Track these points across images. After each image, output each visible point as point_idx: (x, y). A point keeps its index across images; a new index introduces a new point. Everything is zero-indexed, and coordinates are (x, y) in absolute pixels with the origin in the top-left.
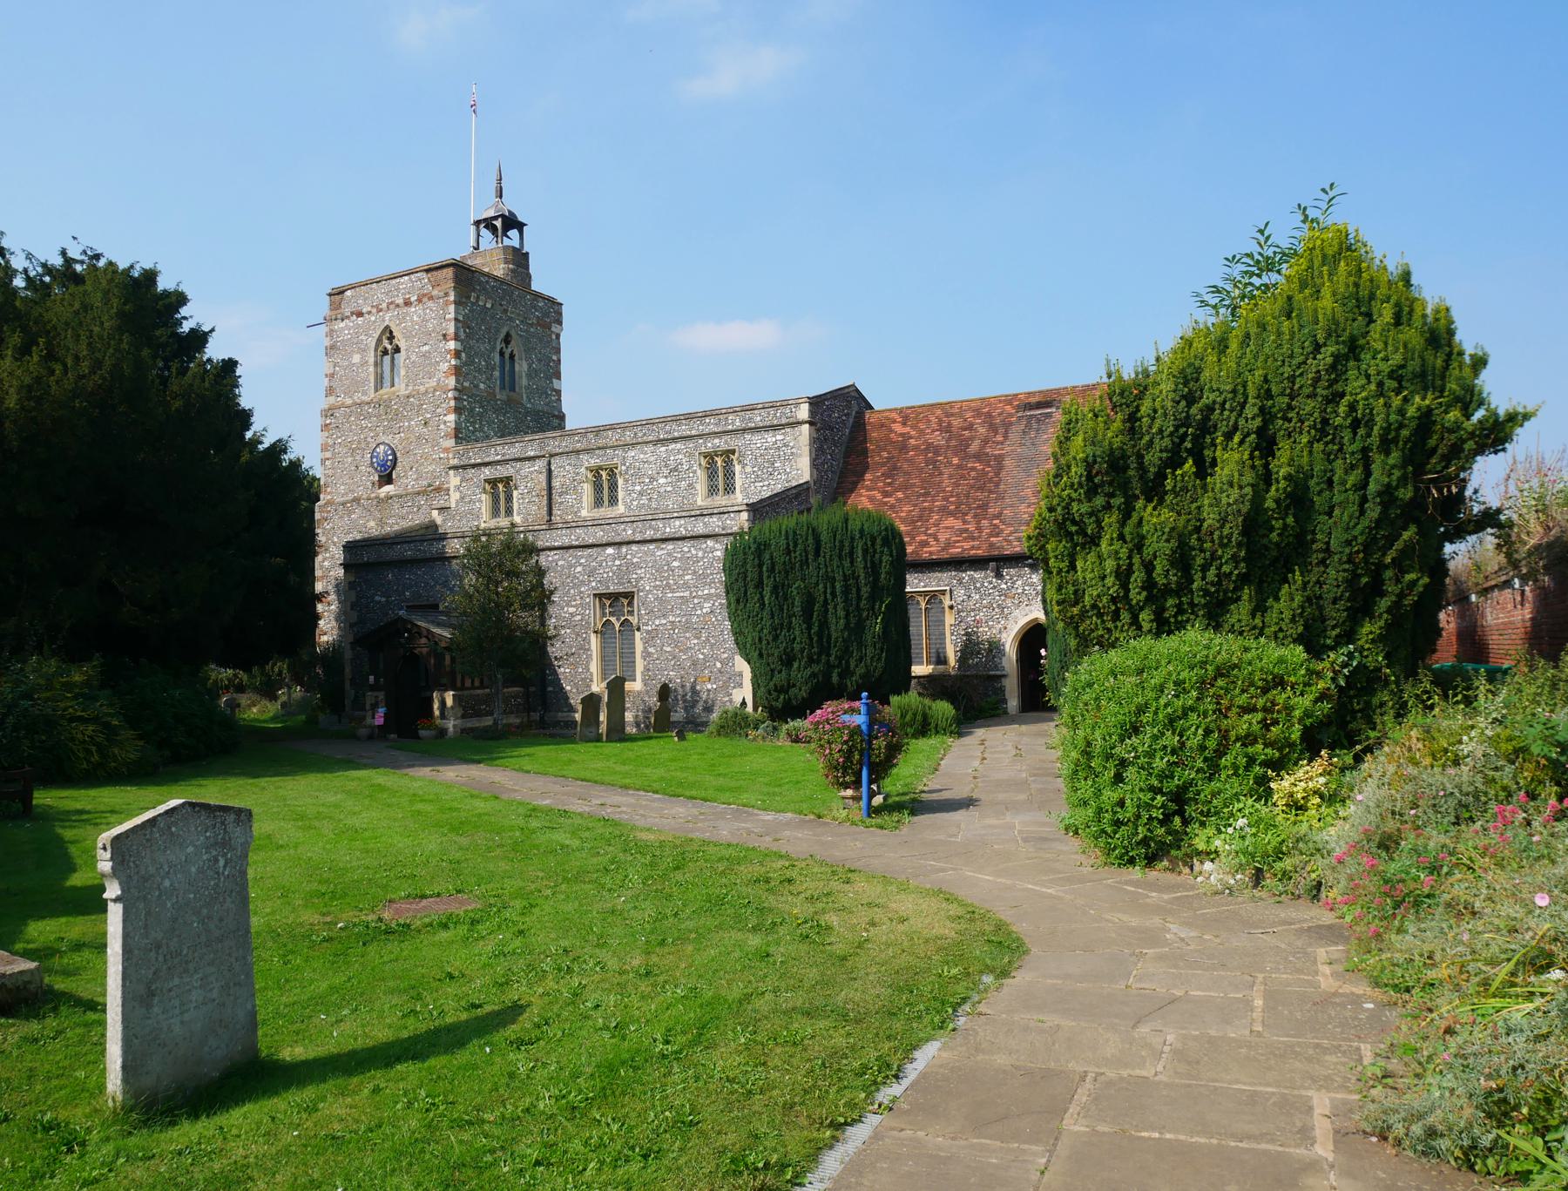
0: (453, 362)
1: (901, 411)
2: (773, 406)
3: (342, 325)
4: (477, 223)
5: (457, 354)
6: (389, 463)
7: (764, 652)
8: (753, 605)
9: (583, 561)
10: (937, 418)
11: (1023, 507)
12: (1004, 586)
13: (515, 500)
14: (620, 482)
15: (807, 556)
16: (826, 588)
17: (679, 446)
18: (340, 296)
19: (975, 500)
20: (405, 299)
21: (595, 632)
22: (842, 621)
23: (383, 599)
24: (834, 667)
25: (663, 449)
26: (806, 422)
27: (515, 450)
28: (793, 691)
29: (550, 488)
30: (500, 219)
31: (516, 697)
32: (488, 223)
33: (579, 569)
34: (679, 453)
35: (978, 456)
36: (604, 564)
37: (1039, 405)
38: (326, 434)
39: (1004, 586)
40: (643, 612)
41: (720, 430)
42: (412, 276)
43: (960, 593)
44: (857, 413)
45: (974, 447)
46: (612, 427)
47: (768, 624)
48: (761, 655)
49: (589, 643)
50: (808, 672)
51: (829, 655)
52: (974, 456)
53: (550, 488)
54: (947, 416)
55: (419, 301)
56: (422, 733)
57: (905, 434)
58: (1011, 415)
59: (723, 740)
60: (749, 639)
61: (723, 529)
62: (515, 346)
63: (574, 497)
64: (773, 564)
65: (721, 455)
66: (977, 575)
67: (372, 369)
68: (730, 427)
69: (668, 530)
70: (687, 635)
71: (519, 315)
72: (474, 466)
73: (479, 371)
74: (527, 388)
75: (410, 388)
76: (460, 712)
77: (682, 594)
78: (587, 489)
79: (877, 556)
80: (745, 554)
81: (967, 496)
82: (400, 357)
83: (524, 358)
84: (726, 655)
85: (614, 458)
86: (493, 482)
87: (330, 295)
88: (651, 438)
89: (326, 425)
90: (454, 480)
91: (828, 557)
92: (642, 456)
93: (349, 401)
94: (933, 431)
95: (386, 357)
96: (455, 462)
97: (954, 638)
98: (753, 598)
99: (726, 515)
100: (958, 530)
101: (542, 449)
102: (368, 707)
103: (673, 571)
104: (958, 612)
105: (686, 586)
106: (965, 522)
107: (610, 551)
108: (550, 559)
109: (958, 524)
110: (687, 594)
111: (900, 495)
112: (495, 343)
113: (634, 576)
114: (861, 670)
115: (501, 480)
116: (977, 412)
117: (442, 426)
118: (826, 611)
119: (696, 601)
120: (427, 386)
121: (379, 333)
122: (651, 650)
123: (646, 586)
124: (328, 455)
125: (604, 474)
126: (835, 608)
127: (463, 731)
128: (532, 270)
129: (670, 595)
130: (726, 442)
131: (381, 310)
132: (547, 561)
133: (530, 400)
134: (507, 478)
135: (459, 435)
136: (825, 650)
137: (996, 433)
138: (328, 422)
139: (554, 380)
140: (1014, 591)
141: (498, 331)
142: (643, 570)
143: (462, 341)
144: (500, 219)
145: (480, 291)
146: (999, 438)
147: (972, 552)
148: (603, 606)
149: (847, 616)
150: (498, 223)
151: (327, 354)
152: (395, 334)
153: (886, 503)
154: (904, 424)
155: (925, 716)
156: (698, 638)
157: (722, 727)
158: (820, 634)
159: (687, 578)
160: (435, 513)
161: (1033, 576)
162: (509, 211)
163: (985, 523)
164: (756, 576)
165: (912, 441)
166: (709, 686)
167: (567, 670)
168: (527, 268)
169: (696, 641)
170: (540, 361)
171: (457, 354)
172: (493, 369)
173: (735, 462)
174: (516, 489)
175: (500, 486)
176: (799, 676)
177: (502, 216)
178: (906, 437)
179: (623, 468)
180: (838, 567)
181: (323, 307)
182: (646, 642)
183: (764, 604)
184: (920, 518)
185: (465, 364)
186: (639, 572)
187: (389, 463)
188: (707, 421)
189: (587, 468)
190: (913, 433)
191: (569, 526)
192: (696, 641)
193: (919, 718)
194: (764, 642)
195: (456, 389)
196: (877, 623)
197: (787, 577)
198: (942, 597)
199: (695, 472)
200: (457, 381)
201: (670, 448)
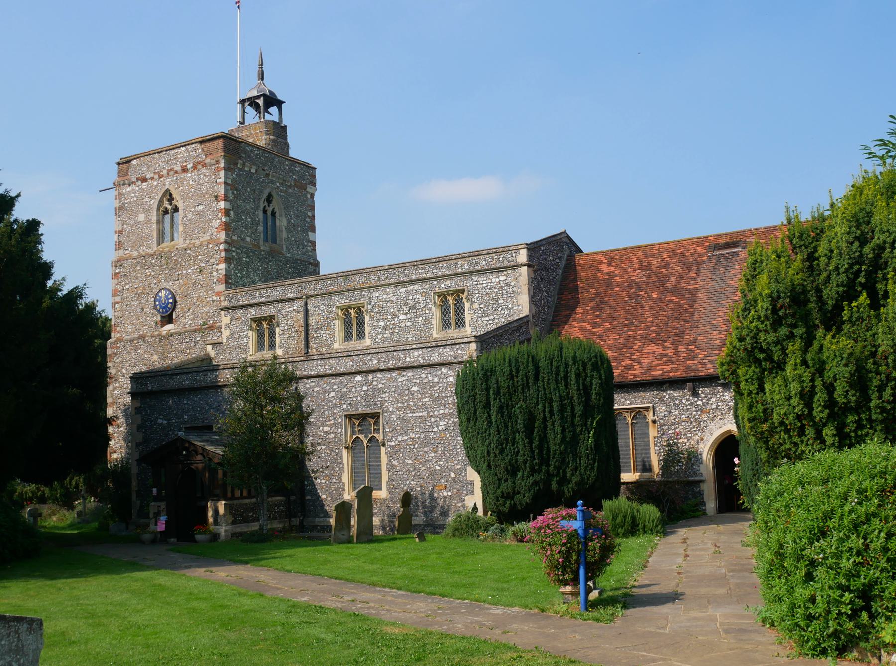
0: (224, 219)
1: (606, 253)
2: (497, 251)
3: (129, 189)
4: (243, 102)
5: (227, 212)
6: (169, 306)
7: (493, 464)
8: (482, 423)
9: (335, 387)
10: (637, 258)
11: (715, 335)
12: (700, 403)
13: (277, 336)
14: (367, 318)
15: (527, 380)
16: (545, 408)
17: (416, 287)
18: (127, 165)
19: (673, 329)
20: (182, 167)
21: (347, 448)
22: (559, 436)
23: (165, 422)
24: (553, 476)
25: (403, 290)
26: (525, 265)
27: (277, 294)
28: (518, 498)
29: (307, 325)
30: (262, 98)
31: (278, 505)
32: (252, 102)
33: (332, 394)
34: (416, 293)
35: (675, 291)
36: (354, 389)
37: (727, 245)
38: (116, 281)
39: (700, 403)
40: (387, 430)
41: (451, 273)
42: (188, 147)
43: (662, 410)
44: (568, 256)
45: (671, 282)
46: (359, 272)
47: (495, 440)
48: (489, 466)
49: (341, 457)
50: (531, 480)
51: (548, 465)
52: (671, 291)
53: (307, 325)
54: (646, 257)
55: (195, 168)
56: (199, 537)
57: (610, 273)
58: (702, 255)
59: (458, 541)
60: (479, 453)
61: (455, 358)
62: (276, 205)
63: (327, 332)
64: (498, 388)
65: (453, 295)
66: (676, 394)
67: (154, 226)
68: (460, 270)
69: (408, 359)
70: (426, 449)
71: (279, 178)
72: (242, 307)
73: (246, 226)
74: (288, 239)
75: (188, 241)
76: (230, 518)
77: (420, 414)
78: (338, 325)
79: (588, 379)
80: (474, 379)
81: (666, 325)
82: (179, 216)
83: (283, 213)
84: (459, 467)
85: (361, 298)
86: (258, 321)
87: (119, 164)
88: (392, 281)
89: (116, 274)
90: (225, 319)
91: (546, 381)
92: (385, 296)
93: (135, 254)
94: (635, 270)
95: (166, 216)
96: (226, 304)
97: (657, 448)
98: (481, 417)
99: (458, 346)
100: (658, 355)
101: (300, 291)
102: (151, 515)
103: (412, 395)
104: (661, 426)
105: (424, 407)
106: (664, 348)
107: (359, 378)
108: (308, 385)
109: (658, 350)
110: (425, 414)
111: (607, 325)
112: (259, 203)
113: (380, 399)
114: (576, 479)
115: (265, 319)
116: (673, 253)
117: (215, 274)
118: (545, 428)
119: (433, 420)
120: (201, 239)
121: (160, 195)
122: (395, 463)
123: (390, 408)
124: (118, 299)
125: (352, 312)
126: (553, 424)
127: (234, 535)
128: (288, 141)
129: (410, 415)
130: (456, 283)
131: (162, 176)
132: (305, 387)
133: (289, 250)
134: (269, 316)
135: (229, 281)
136: (545, 461)
137: (690, 271)
138: (118, 271)
139: (310, 233)
141: (261, 192)
142: (387, 394)
143: (231, 201)
144: (262, 98)
145: (245, 158)
146: (693, 275)
147: (672, 374)
148: (353, 426)
149: (563, 431)
150: (261, 101)
151: (116, 214)
152: (174, 196)
153: (595, 333)
154: (609, 264)
155: (634, 518)
156: (435, 452)
157: (456, 529)
158: (540, 448)
159: (425, 400)
160: (209, 348)
161: (726, 394)
162: (270, 91)
163: (682, 348)
164: (484, 399)
165: (617, 279)
166: (445, 494)
167: (323, 481)
168: (285, 138)
169: (433, 455)
170: (297, 216)
171: (227, 212)
172: (258, 224)
173: (465, 301)
174: (278, 326)
175: (265, 324)
176: (523, 484)
177: (264, 95)
178: (612, 275)
179: (369, 307)
180: (554, 389)
181: (113, 174)
182: (390, 456)
183: (491, 422)
184: (625, 345)
185: (234, 221)
186: (384, 396)
187: (169, 306)
188: (440, 265)
189: (338, 308)
190: (617, 272)
191: (323, 357)
192: (433, 455)
193: (628, 519)
194: (492, 455)
195: (226, 242)
196: (589, 437)
197: (511, 399)
198: (646, 413)
199: (430, 309)
200: (227, 235)
201: (409, 289)
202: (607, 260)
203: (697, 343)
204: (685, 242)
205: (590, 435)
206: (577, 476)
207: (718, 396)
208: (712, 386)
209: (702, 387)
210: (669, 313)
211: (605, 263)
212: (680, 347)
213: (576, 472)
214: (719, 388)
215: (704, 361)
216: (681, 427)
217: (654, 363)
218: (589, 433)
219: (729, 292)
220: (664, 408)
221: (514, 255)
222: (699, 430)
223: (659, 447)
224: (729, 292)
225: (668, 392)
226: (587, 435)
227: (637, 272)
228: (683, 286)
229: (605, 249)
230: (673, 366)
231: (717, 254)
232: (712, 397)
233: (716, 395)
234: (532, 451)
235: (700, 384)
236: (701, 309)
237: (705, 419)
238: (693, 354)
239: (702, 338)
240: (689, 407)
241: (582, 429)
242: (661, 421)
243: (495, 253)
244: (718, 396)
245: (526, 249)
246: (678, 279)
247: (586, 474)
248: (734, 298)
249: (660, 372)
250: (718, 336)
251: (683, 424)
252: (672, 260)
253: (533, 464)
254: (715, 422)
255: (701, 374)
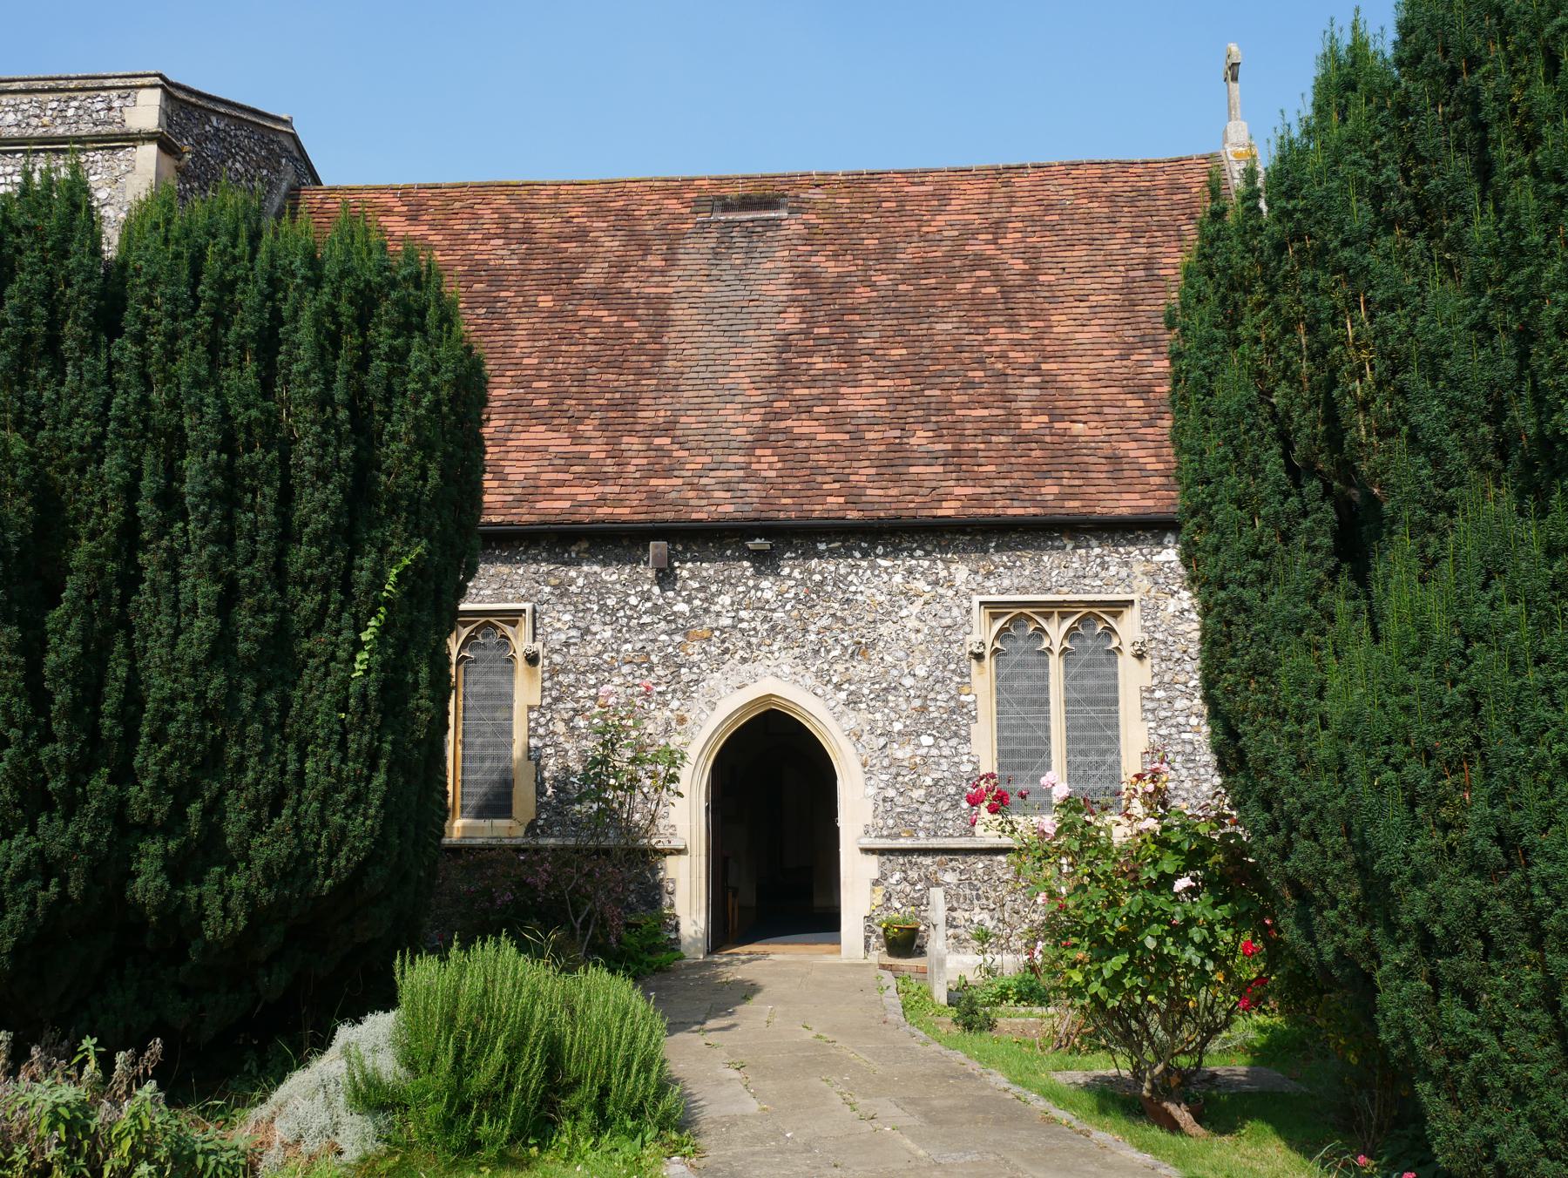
1: (404, 192)
2: (55, 87)
11: (730, 413)
12: (681, 607)
15: (54, 324)
16: (137, 475)
19: (603, 389)
22: (202, 627)
24: (147, 829)
35: (603, 296)
37: (746, 203)
39: (681, 607)
43: (560, 622)
45: (593, 275)
51: (125, 775)
52: (595, 295)
54: (519, 210)
57: (414, 238)
58: (681, 219)
66: (610, 575)
79: (379, 367)
81: (581, 380)
91: (156, 341)
94: (488, 237)
100: (558, 455)
104: (554, 672)
106: (576, 439)
109: (559, 442)
114: (269, 849)
116: (598, 207)
118: (131, 580)
126: (172, 563)
137: (646, 251)
140: (709, 621)
146: (655, 262)
147: (603, 511)
149: (227, 602)
154: (413, 218)
155: (554, 1052)
161: (765, 584)
163: (632, 443)
180: (198, 383)
190: (435, 238)
193: (532, 1065)
198: (509, 630)
202: (405, 208)
203: (678, 433)
204: (628, 185)
205: (365, 637)
206: (280, 835)
207: (741, 589)
208: (723, 558)
209: (693, 560)
210: (589, 348)
211: (400, 214)
212: (625, 439)
213: (276, 812)
214: (746, 564)
215: (704, 481)
216: (617, 680)
217: (544, 476)
218: (359, 628)
219: (760, 309)
220: (567, 617)
221: (116, 104)
222: (674, 691)
223: (541, 737)
224: (760, 309)
225: (585, 568)
226: (348, 634)
227: (492, 242)
228: (627, 285)
229: (401, 182)
230: (607, 489)
231: (719, 221)
232: (720, 593)
233: (735, 586)
234: (39, 697)
235: (686, 549)
236: (683, 346)
237: (696, 658)
238: (666, 461)
239: (693, 420)
240: (646, 619)
241: (324, 605)
242: (557, 658)
243: (50, 90)
244: (741, 589)
245: (158, 91)
246: (614, 270)
247: (324, 824)
248: (778, 327)
249: (567, 504)
250: (740, 418)
251: (626, 669)
252: (595, 225)
253: (36, 766)
254: (726, 668)
255: (694, 516)
